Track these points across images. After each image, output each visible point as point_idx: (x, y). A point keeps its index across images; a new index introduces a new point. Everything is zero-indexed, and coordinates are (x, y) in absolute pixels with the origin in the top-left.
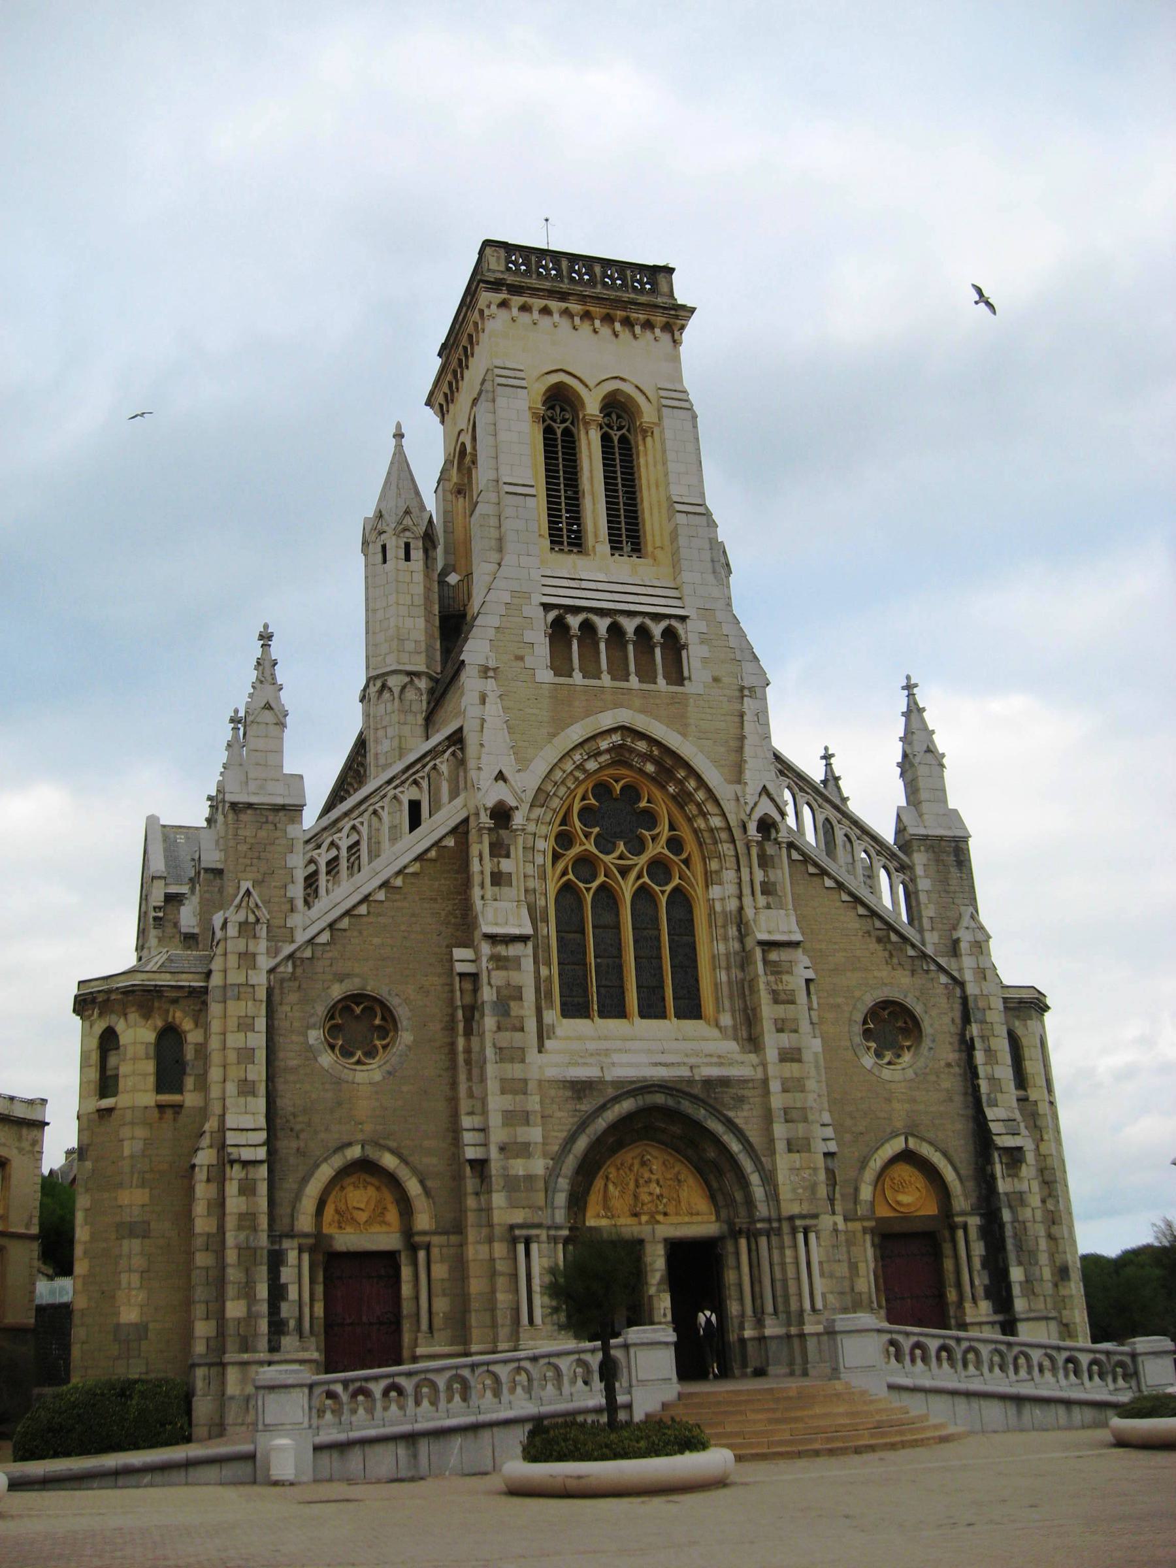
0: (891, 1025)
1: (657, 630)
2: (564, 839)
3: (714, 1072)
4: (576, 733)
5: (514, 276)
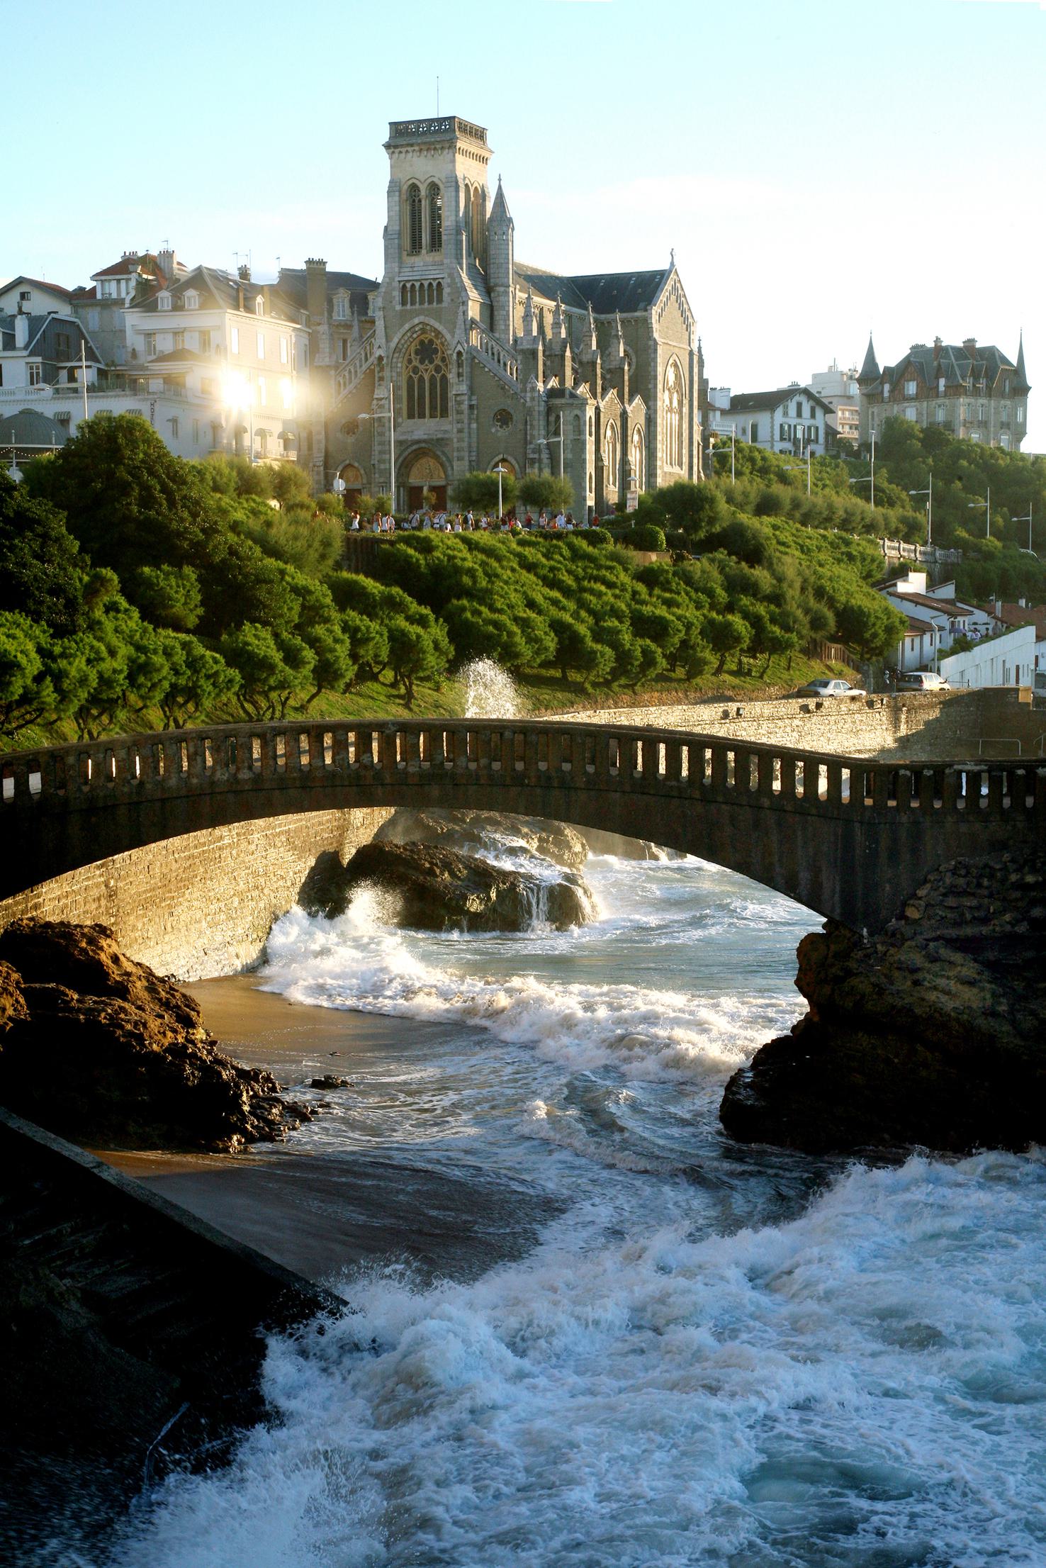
0: (504, 418)
1: (435, 284)
2: (410, 361)
3: (440, 436)
4: (407, 326)
5: (405, 137)
